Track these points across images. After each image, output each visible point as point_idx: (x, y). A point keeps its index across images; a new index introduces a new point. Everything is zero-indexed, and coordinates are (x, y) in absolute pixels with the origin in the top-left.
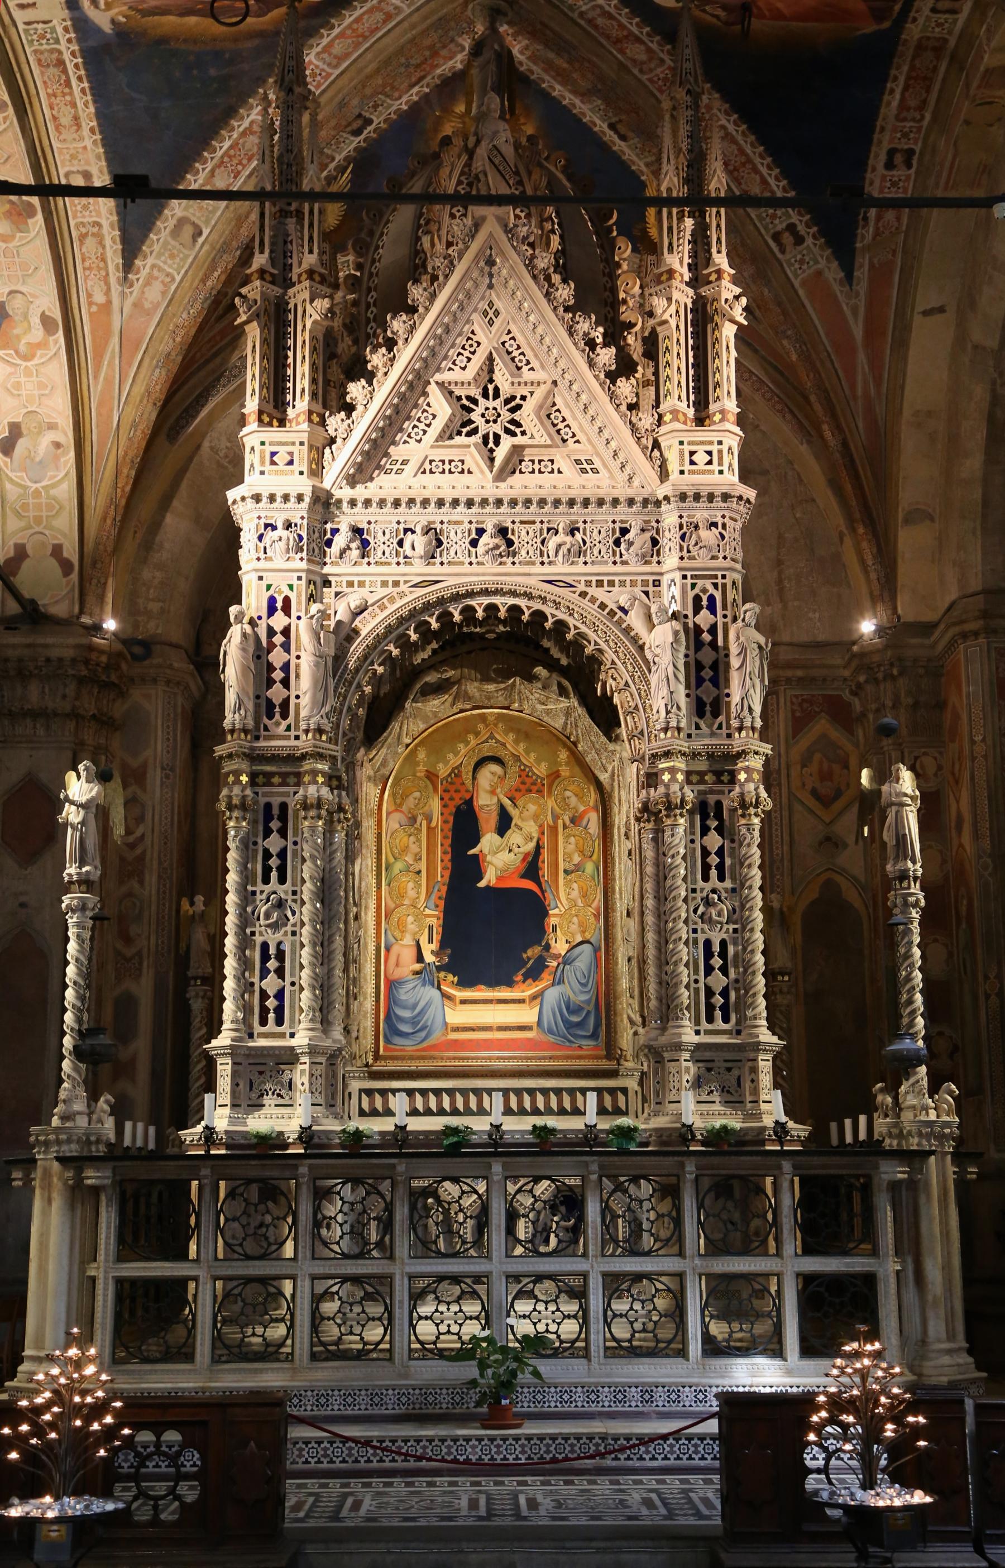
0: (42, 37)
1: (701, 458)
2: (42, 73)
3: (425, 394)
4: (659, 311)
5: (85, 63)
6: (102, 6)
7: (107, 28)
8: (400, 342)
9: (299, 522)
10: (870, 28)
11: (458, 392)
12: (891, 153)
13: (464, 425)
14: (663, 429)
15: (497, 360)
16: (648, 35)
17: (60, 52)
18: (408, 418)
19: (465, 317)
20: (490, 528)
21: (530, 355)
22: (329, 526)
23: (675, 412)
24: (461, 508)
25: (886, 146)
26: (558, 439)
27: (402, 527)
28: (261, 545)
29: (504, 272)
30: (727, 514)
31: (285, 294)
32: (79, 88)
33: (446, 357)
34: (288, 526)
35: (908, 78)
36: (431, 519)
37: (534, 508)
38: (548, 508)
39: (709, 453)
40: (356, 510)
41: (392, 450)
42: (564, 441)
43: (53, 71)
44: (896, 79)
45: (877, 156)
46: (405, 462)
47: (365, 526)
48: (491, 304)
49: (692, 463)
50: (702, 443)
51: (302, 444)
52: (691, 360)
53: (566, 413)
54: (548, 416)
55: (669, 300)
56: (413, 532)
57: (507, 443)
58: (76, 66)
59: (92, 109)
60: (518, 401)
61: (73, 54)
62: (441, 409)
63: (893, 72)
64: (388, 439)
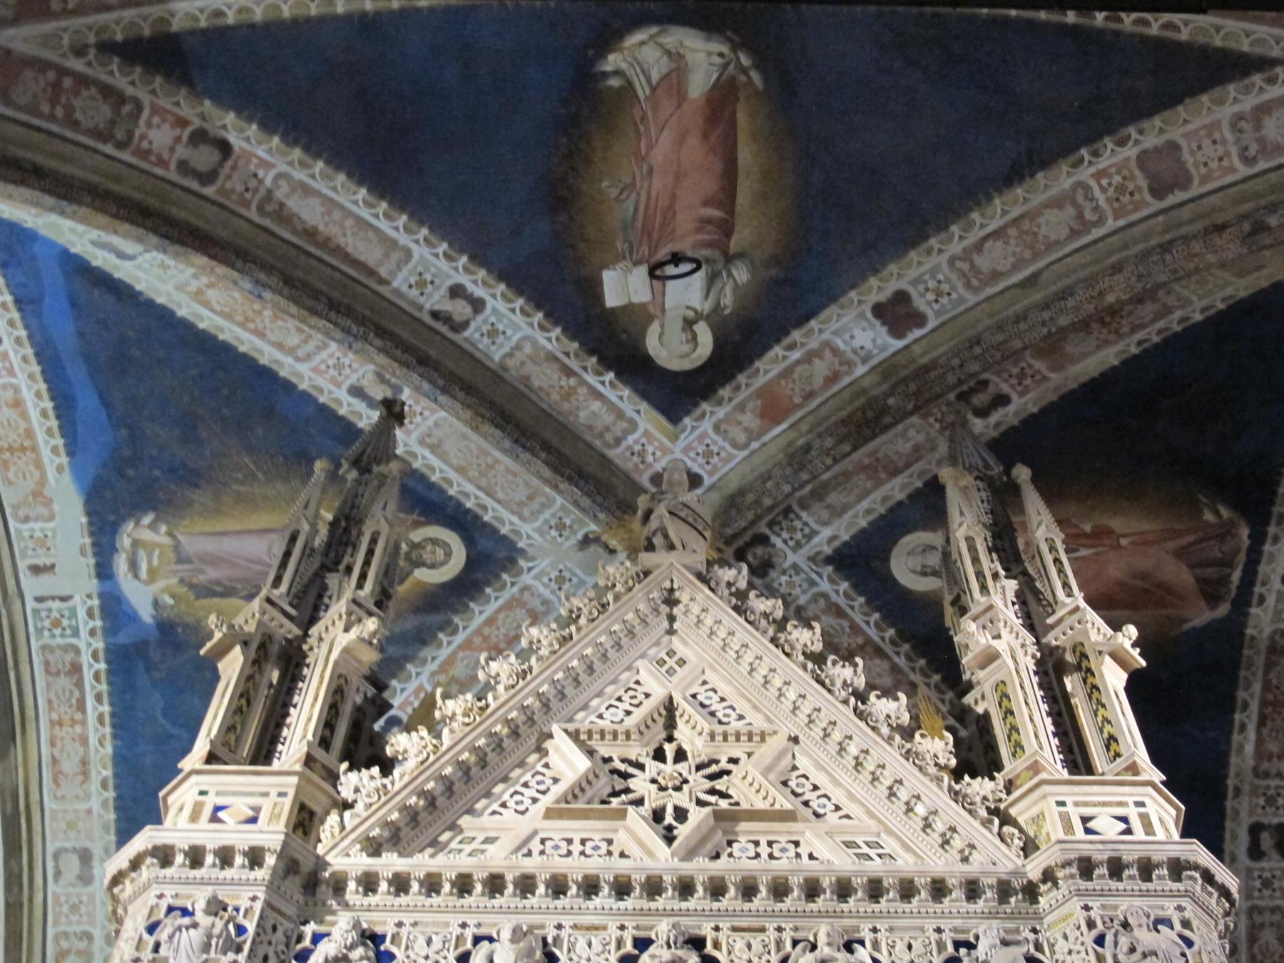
0: (57, 623)
1: (1108, 827)
2: (48, 685)
3: (542, 752)
4: (983, 641)
5: (109, 672)
6: (144, 567)
7: (146, 614)
8: (501, 688)
9: (244, 904)
10: (1201, 616)
11: (604, 751)
12: (1256, 830)
13: (615, 794)
14: (1016, 794)
15: (682, 704)
16: (893, 642)
17: (77, 651)
18: (505, 779)
19: (625, 661)
20: (662, 929)
21: (742, 706)
22: (309, 929)
23: (1035, 768)
24: (604, 899)
25: (1246, 821)
26: (807, 813)
27: (468, 934)
28: (150, 941)
29: (696, 609)
30: (1185, 902)
31: (306, 635)
32: (97, 710)
33: (585, 707)
34: (216, 907)
35: (1264, 704)
36: (535, 919)
37: (762, 900)
38: (793, 901)
39: (1124, 819)
40: (373, 899)
41: (465, 821)
42: (817, 815)
43: (64, 682)
44: (1245, 706)
45: (1235, 837)
46: (488, 841)
47: (390, 930)
48: (671, 653)
49: (1088, 831)
50: (1104, 804)
51: (281, 794)
52: (1051, 728)
53: (817, 777)
54: (785, 783)
55: (998, 637)
56: (491, 940)
57: (697, 815)
58: (97, 676)
59: (109, 749)
60: (724, 765)
61: (95, 655)
62: (567, 761)
63: (1241, 695)
64: (460, 805)
